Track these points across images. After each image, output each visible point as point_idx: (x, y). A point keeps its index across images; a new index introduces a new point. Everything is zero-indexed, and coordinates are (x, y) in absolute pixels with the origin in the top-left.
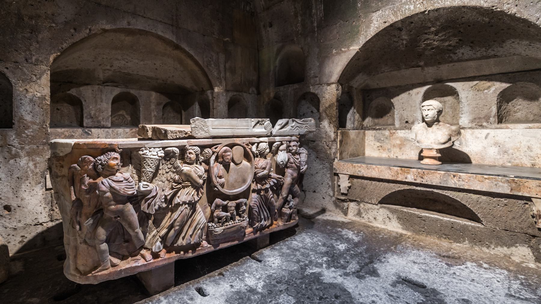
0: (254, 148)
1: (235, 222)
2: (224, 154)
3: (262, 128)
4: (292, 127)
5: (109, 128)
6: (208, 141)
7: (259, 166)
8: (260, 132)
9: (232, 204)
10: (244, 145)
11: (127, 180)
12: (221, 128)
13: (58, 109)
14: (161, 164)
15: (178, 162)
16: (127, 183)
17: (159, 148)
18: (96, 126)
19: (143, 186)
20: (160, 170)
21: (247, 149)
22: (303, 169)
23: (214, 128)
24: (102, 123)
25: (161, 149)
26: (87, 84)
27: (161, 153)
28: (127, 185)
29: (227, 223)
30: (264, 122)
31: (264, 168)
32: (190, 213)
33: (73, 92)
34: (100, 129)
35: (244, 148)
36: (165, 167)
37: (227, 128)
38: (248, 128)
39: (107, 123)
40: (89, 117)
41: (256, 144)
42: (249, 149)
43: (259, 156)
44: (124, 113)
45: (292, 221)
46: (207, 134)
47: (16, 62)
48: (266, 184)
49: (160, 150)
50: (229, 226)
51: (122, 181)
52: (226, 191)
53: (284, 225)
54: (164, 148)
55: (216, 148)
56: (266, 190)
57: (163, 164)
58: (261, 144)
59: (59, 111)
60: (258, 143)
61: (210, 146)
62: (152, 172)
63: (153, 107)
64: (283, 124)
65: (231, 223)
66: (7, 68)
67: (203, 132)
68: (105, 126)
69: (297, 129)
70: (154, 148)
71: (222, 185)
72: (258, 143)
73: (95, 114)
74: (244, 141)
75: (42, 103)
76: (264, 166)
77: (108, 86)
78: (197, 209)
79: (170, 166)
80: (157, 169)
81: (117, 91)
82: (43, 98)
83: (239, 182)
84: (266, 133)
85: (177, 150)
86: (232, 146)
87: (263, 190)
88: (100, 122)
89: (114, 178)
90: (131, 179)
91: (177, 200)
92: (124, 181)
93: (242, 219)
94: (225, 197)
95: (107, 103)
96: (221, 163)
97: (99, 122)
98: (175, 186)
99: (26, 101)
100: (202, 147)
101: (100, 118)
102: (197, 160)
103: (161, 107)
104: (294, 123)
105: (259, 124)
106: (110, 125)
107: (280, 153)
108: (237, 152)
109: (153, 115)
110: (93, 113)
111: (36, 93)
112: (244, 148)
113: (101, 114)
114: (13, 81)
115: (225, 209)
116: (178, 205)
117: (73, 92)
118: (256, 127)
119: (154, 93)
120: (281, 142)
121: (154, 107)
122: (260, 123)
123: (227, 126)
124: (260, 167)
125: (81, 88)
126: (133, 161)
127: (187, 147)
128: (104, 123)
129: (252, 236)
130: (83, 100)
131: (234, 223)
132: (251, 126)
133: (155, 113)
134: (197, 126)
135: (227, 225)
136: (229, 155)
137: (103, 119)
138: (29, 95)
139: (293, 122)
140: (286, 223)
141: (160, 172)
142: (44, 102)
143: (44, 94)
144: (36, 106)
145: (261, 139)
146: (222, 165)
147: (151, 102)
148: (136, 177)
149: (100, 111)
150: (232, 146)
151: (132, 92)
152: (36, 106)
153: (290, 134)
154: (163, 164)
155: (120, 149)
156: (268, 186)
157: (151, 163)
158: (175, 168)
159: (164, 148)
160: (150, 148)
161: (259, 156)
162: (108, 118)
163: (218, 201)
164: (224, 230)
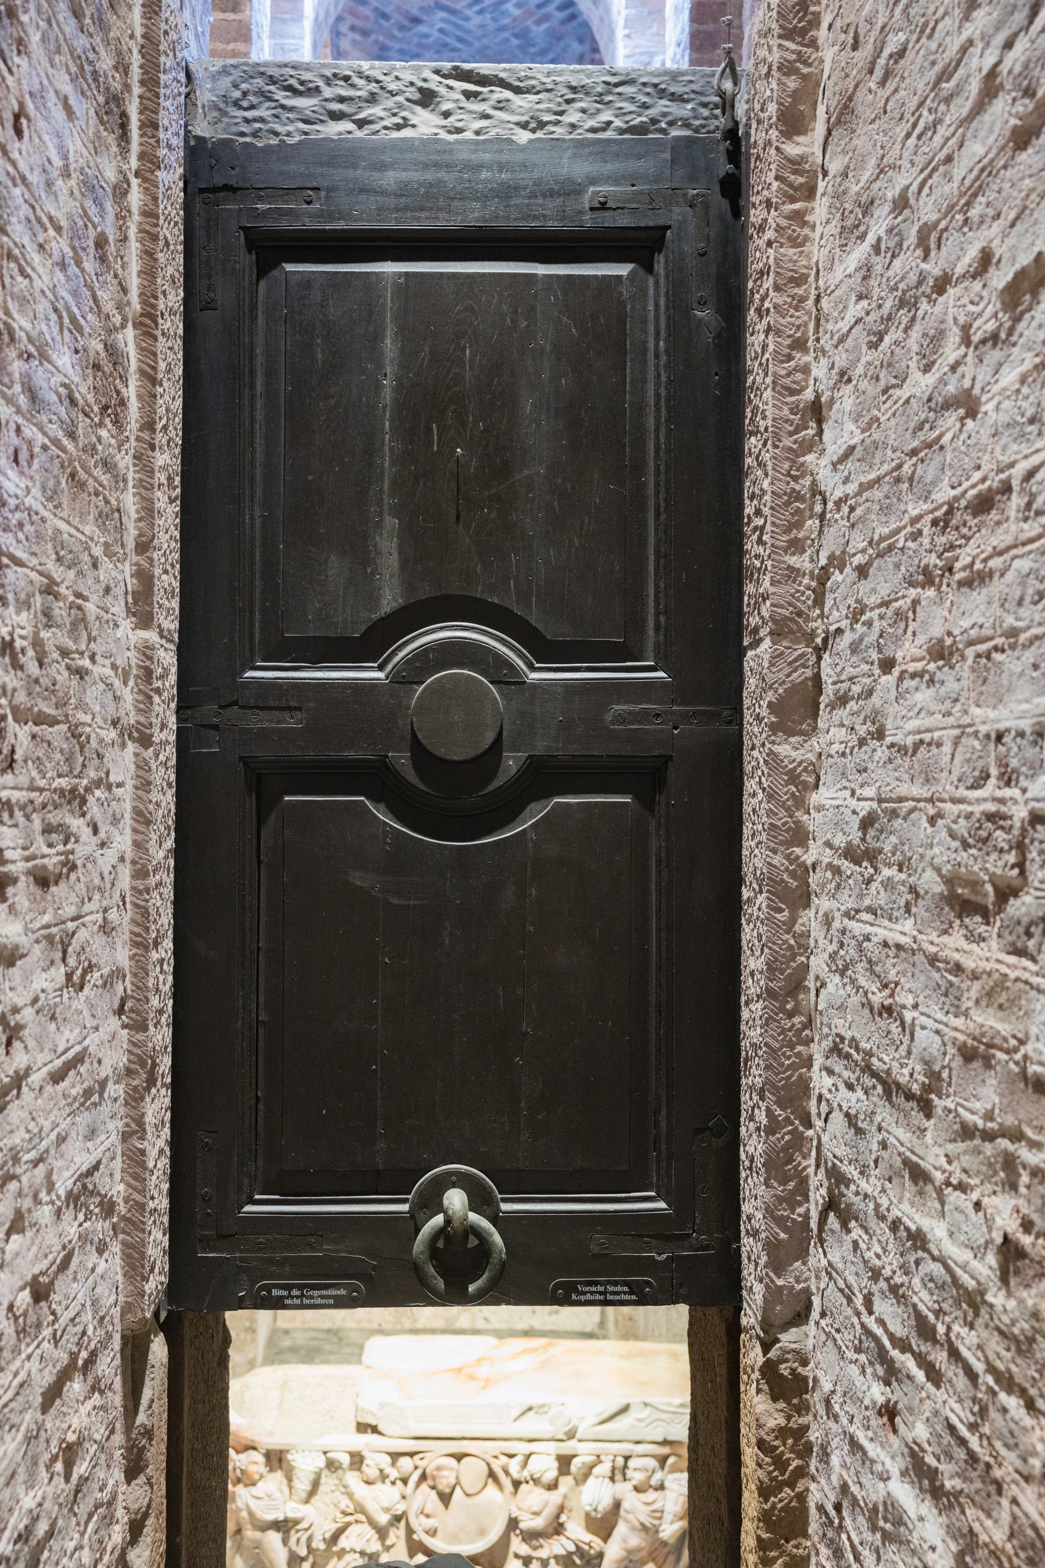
4: (639, 1420)
7: (525, 1505)
15: (352, 1479)
19: (292, 1509)
31: (537, 1514)
35: (488, 1465)
36: (328, 1482)
48: (541, 1546)
54: (325, 1453)
61: (412, 1455)
71: (433, 1533)
76: (536, 1509)
79: (337, 1482)
80: (316, 1485)
86: (459, 1457)
89: (253, 1490)
90: (278, 1494)
91: (343, 1542)
96: (433, 1488)
100: (395, 1456)
102: (383, 1477)
105: (531, 1413)
107: (591, 1480)
108: (472, 1471)
112: (488, 1465)
116: (343, 1552)
126: (284, 1465)
127: (365, 1453)
148: (286, 1489)
150: (459, 1457)
156: (543, 1553)
158: (345, 1487)
159: (325, 1453)
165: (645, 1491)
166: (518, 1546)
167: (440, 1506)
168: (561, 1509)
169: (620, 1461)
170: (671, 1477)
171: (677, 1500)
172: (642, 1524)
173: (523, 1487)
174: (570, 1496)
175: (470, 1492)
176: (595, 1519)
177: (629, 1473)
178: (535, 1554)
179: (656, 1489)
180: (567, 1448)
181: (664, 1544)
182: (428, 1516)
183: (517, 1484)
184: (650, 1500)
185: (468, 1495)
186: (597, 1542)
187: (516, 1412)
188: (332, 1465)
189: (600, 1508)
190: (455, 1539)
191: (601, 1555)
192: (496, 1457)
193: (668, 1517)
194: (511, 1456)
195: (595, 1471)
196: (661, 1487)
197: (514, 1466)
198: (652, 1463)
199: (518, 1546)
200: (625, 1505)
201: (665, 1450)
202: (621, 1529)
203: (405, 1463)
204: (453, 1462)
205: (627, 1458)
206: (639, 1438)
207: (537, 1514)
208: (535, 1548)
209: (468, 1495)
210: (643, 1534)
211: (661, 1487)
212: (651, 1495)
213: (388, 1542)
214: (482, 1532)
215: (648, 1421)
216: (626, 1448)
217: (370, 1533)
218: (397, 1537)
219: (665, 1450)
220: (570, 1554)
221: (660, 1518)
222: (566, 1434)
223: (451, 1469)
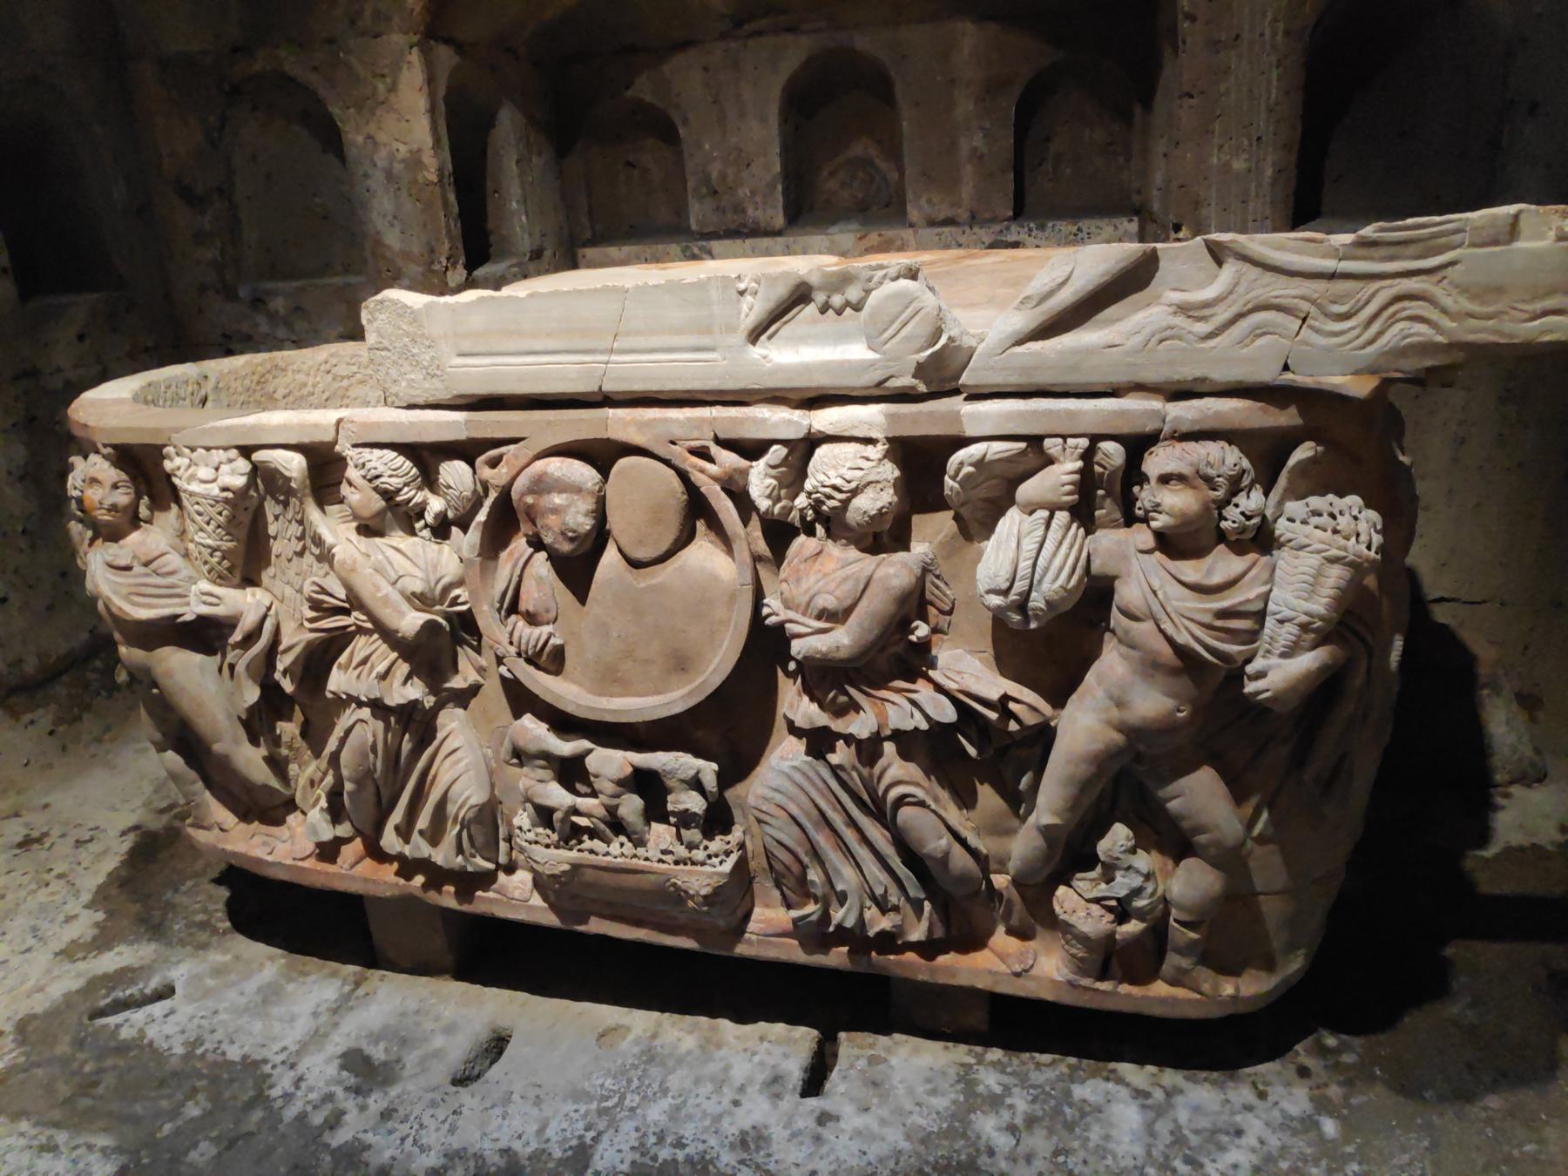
0: (760, 480)
1: (641, 851)
2: (530, 500)
3: (842, 338)
4: (1184, 309)
5: (779, 233)
6: (439, 425)
7: (800, 592)
8: (807, 368)
9: (609, 763)
10: (679, 454)
11: (146, 565)
12: (511, 345)
13: (631, 165)
14: (270, 518)
16: (147, 575)
17: (226, 449)
18: (733, 226)
20: (275, 538)
21: (698, 478)
22: (1261, 675)
23: (466, 346)
24: (750, 212)
25: (234, 453)
26: (683, 45)
27: (233, 472)
28: (146, 585)
29: (597, 844)
30: (853, 293)
31: (835, 617)
32: (406, 746)
33: (643, 89)
34: (739, 242)
35: (683, 476)
37: (552, 344)
38: (705, 341)
39: (770, 212)
40: (704, 190)
41: (777, 453)
42: (715, 479)
43: (820, 530)
44: (873, 152)
45: (1160, 988)
46: (437, 383)
47: (331, 41)
48: (857, 708)
49: (230, 461)
50: (600, 860)
51: (128, 568)
52: (563, 691)
53: (1070, 983)
54: (246, 451)
55: (494, 463)
56: (869, 750)
57: (277, 518)
58: (822, 452)
59: (636, 173)
60: (811, 442)
61: (467, 451)
62: (209, 547)
63: (965, 106)
64: (1066, 297)
65: (617, 851)
66: (315, 69)
67: (417, 376)
68: (763, 225)
69: (1260, 332)
70: (208, 449)
72: (811, 442)
73: (723, 176)
74: (677, 432)
75: (416, 181)
76: (828, 601)
77: (760, 33)
78: (440, 736)
81: (794, 53)
82: (414, 162)
83: (647, 662)
84: (877, 376)
85: (293, 465)
87: (849, 739)
88: (744, 211)
90: (174, 560)
92: (138, 569)
93: (681, 851)
94: (564, 723)
95: (763, 119)
97: (739, 209)
98: (311, 620)
99: (377, 180)
101: (743, 192)
102: (405, 517)
103: (1009, 104)
104: (1230, 269)
105: (810, 310)
106: (779, 221)
107: (1011, 522)
109: (964, 147)
110: (715, 170)
111: (396, 145)
112: (683, 476)
113: (744, 174)
114: (335, 110)
115: (571, 773)
117: (643, 89)
118: (787, 329)
119: (969, 25)
120: (1035, 441)
121: (971, 107)
122: (820, 298)
123: (549, 335)
124: (804, 599)
125: (666, 68)
128: (759, 213)
129: (792, 952)
130: (677, 120)
131: (635, 856)
132: (731, 329)
133: (978, 141)
134: (386, 343)
135: (592, 851)
136: (556, 510)
137: (753, 193)
138: (381, 158)
139: (1220, 263)
140: (1086, 982)
141: (276, 547)
142: (421, 180)
143: (415, 147)
144: (404, 193)
145: (826, 419)
146: (543, 555)
147: (953, 81)
149: (742, 160)
151: (863, 42)
152: (404, 193)
153: (1150, 376)
154: (277, 518)
155: (105, 446)
156: (861, 725)
157: (200, 514)
159: (246, 451)
160: (193, 450)
161: (820, 530)
162: (772, 186)
163: (534, 730)
164: (576, 867)
165: (1197, 552)
166: (796, 705)
167: (565, 596)
168: (915, 602)
169: (1112, 452)
170: (1294, 507)
171: (1319, 574)
172: (1180, 651)
173: (802, 545)
174: (943, 568)
175: (641, 554)
176: (1023, 634)
177: (1146, 496)
178: (838, 726)
179: (1239, 548)
180: (926, 419)
181: (1257, 710)
182: (532, 619)
183: (779, 534)
184: (1216, 579)
185: (636, 564)
186: (1028, 702)
187: (752, 310)
188: (266, 480)
189: (1037, 601)
190: (610, 679)
191: (1044, 736)
192: (703, 453)
193: (1277, 633)
194: (752, 450)
195: (1026, 490)
196: (1261, 539)
197: (760, 480)
198: (1226, 458)
199: (796, 705)
200: (1128, 593)
201: (1287, 418)
202: (1111, 664)
203: (454, 472)
204: (581, 472)
205: (1138, 445)
206: (1186, 372)
207: (835, 617)
208: (839, 712)
209: (636, 564)
210: (1184, 683)
211: (1261, 539)
212: (1221, 565)
213: (457, 683)
214: (681, 664)
215: (1223, 314)
216: (1137, 409)
217: (384, 656)
218: (481, 670)
219: (1287, 418)
220: (938, 730)
221: (1253, 636)
222: (920, 371)
223: (577, 490)
